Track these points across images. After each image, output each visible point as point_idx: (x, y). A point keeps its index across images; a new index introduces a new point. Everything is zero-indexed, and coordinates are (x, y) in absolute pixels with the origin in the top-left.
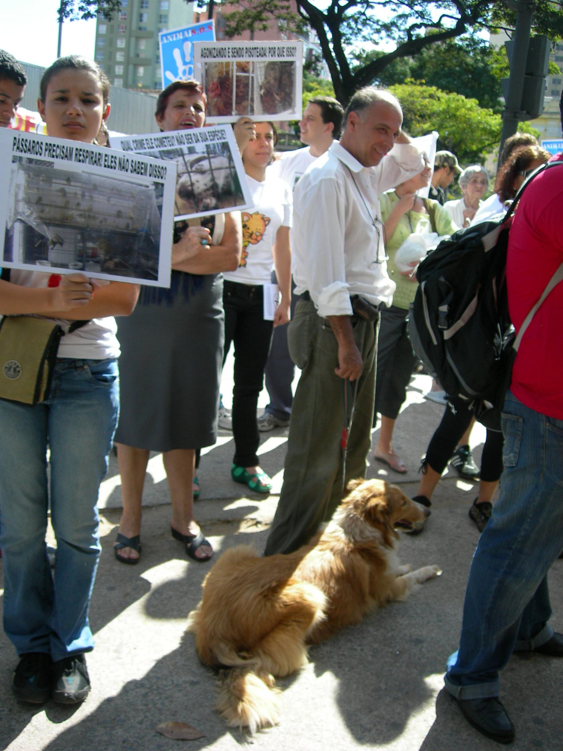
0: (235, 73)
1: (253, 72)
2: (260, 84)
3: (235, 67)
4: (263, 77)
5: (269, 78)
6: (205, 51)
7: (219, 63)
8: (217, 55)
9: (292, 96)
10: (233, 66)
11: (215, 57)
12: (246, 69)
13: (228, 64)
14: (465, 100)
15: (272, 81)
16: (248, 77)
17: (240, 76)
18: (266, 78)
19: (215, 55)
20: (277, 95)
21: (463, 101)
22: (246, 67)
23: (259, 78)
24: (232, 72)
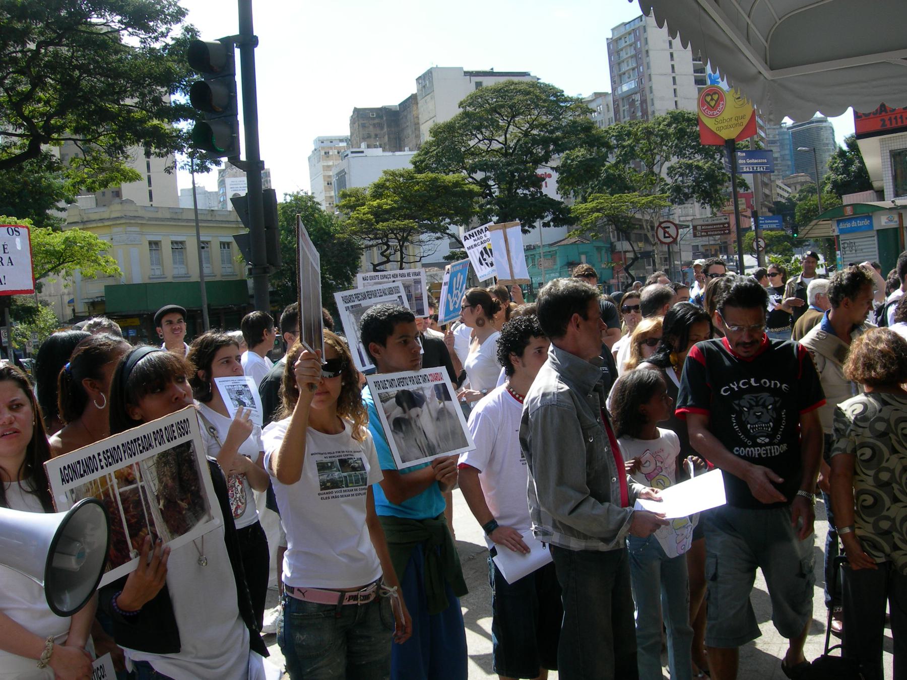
0: (118, 490)
1: (141, 480)
2: (156, 494)
3: (115, 481)
4: (156, 482)
5: (164, 479)
6: (66, 472)
7: (90, 482)
8: (85, 471)
9: (202, 494)
10: (111, 481)
11: (82, 476)
12: (130, 478)
13: (103, 480)
15: (170, 483)
16: (137, 488)
17: (126, 491)
18: (160, 481)
19: (82, 472)
20: (182, 500)
22: (129, 474)
23: (152, 485)
24: (113, 490)
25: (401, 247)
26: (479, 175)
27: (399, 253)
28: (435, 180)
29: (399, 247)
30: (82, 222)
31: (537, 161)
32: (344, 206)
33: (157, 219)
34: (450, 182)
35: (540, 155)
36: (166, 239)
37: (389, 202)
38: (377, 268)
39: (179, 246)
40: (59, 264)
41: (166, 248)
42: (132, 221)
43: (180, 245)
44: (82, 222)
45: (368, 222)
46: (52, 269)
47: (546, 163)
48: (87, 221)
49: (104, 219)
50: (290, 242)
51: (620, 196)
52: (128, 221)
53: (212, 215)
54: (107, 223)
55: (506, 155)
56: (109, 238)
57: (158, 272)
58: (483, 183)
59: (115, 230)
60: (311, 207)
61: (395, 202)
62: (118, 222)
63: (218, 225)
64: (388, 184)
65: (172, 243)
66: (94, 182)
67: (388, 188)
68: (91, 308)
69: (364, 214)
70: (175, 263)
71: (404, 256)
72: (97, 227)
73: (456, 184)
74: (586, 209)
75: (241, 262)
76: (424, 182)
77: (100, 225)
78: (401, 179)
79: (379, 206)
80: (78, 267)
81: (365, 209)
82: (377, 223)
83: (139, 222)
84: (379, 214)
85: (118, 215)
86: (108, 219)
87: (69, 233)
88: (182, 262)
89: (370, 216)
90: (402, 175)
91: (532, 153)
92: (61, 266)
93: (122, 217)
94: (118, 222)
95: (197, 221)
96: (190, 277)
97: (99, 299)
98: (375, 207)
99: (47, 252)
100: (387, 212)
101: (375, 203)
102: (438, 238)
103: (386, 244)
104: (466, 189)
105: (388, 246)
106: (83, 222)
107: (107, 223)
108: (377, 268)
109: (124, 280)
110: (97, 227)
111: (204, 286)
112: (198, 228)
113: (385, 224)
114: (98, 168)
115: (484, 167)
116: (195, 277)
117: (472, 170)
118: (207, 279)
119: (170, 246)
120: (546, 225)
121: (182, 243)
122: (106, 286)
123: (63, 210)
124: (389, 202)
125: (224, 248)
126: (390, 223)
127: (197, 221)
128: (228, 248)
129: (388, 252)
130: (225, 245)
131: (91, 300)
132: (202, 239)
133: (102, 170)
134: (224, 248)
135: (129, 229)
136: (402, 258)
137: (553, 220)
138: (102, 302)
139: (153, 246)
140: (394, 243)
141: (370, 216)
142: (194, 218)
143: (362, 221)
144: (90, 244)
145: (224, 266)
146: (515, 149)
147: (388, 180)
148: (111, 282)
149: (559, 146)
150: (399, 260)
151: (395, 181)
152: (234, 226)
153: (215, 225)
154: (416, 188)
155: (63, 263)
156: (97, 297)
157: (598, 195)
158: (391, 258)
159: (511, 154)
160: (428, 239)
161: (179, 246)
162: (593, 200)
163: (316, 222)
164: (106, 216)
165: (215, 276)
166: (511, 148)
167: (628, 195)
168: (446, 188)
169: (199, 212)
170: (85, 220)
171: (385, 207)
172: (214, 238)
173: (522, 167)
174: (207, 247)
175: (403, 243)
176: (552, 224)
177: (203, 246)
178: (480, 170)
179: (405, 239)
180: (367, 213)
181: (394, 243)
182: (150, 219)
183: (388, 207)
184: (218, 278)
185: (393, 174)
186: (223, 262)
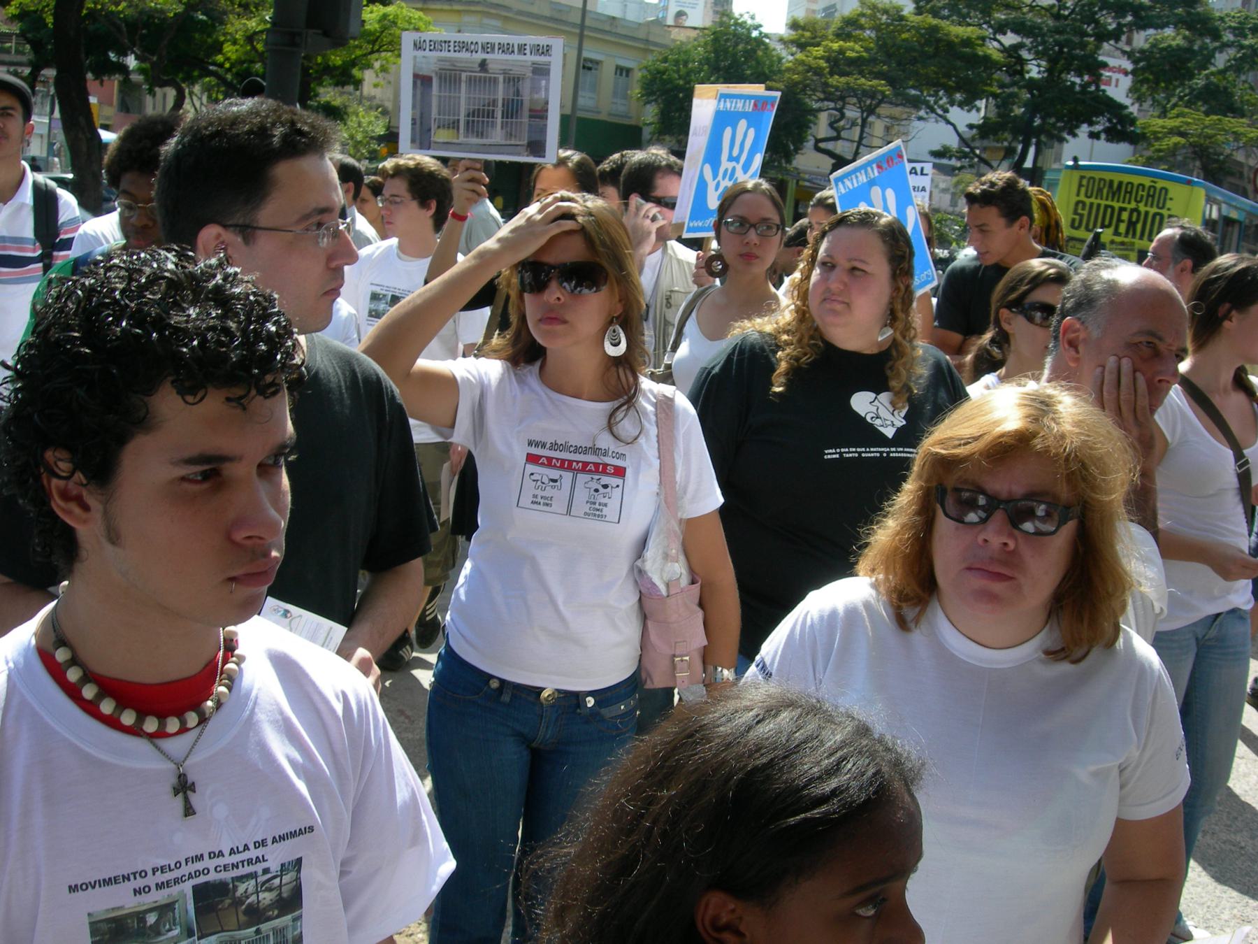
25: (864, 121)
26: (1010, 39)
27: (857, 130)
28: (934, 29)
29: (859, 121)
31: (1103, 36)
32: (792, 42)
33: (530, 15)
34: (957, 37)
35: (1110, 28)
38: (822, 145)
40: (372, 52)
42: (493, 11)
45: (818, 72)
47: (1116, 42)
51: (1219, 120)
52: (486, 9)
53: (611, 24)
55: (1057, 17)
58: (1012, 51)
64: (863, 20)
69: (816, 58)
71: (865, 135)
72: (441, 10)
73: (967, 42)
74: (1163, 127)
76: (917, 29)
78: (885, 17)
79: (841, 51)
81: (818, 51)
82: (832, 74)
84: (837, 63)
89: (823, 64)
90: (886, 12)
91: (1097, 22)
92: (375, 56)
95: (582, 26)
98: (834, 51)
101: (835, 46)
103: (841, 110)
104: (980, 53)
105: (843, 116)
108: (822, 145)
110: (441, 10)
112: (581, 37)
113: (843, 80)
115: (1019, 28)
117: (1001, 28)
118: (580, 114)
120: (1094, 136)
124: (857, 47)
125: (621, 74)
126: (850, 79)
127: (582, 26)
129: (842, 123)
130: (623, 71)
132: (586, 54)
134: (621, 74)
135: (486, 21)
136: (861, 138)
137: (1107, 131)
140: (852, 113)
141: (823, 64)
142: (578, 21)
143: (810, 69)
145: (615, 101)
146: (1073, 11)
147: (863, 15)
149: (1141, 18)
150: (857, 139)
151: (873, 17)
152: (642, 46)
154: (904, 36)
155: (378, 51)
157: (1186, 110)
158: (843, 134)
159: (1066, 18)
162: (1178, 116)
163: (758, 63)
165: (599, 113)
166: (1068, 8)
167: (1232, 120)
168: (950, 44)
171: (850, 54)
173: (1076, 39)
174: (596, 69)
175: (867, 117)
176: (1103, 136)
178: (1013, 31)
179: (871, 111)
180: (820, 58)
181: (852, 113)
182: (520, 13)
184: (603, 117)
185: (874, 7)
186: (615, 94)
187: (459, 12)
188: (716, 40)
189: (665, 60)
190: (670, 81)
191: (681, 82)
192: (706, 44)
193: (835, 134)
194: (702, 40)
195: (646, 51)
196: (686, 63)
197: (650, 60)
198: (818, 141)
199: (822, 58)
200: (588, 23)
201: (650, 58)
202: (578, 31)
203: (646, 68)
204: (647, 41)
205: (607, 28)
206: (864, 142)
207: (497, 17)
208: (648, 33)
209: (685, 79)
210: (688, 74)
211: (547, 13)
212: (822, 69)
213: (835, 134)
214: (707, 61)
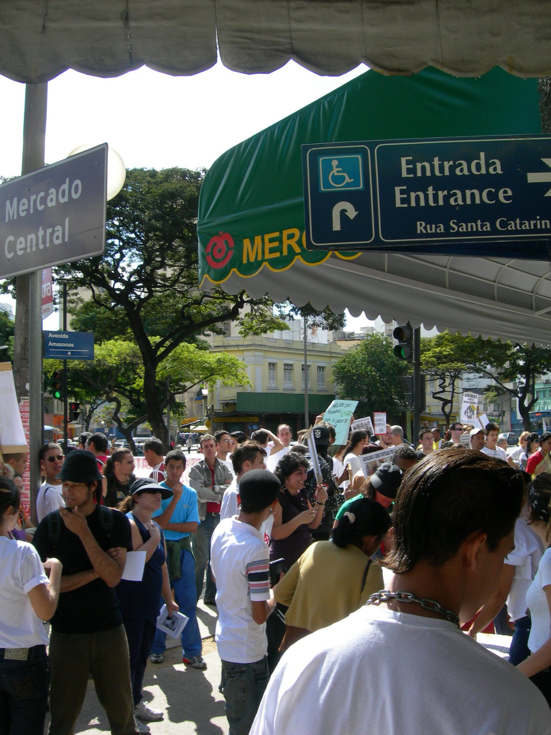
14: (189, 345)
21: (187, 347)
29: (451, 382)
30: (224, 346)
33: (275, 347)
36: (281, 360)
37: (447, 349)
38: (436, 395)
39: (288, 367)
41: (280, 368)
43: (289, 366)
44: (224, 346)
46: (205, 378)
48: (227, 346)
49: (239, 345)
50: (370, 371)
53: (313, 347)
54: (241, 349)
56: (242, 359)
57: (273, 385)
59: (246, 353)
60: (386, 345)
61: (452, 350)
62: (249, 348)
63: (317, 354)
65: (285, 365)
66: (258, 329)
67: (446, 339)
68: (225, 408)
70: (285, 379)
71: (455, 388)
75: (333, 382)
77: (236, 349)
79: (440, 352)
80: (222, 377)
82: (439, 364)
83: (264, 349)
85: (250, 343)
86: (242, 346)
87: (219, 355)
88: (290, 379)
93: (251, 345)
94: (249, 348)
95: (305, 350)
96: (295, 390)
97: (232, 401)
99: (205, 368)
100: (445, 357)
101: (437, 350)
102: (480, 377)
106: (225, 347)
107: (241, 349)
108: (436, 395)
109: (249, 390)
110: (234, 351)
111: (307, 399)
112: (306, 355)
113: (443, 365)
114: (262, 321)
116: (299, 391)
118: (309, 393)
119: (283, 367)
121: (291, 365)
122: (238, 393)
123: (208, 335)
125: (320, 371)
127: (305, 350)
128: (323, 371)
130: (321, 369)
131: (226, 402)
132: (308, 363)
133: (263, 321)
134: (320, 371)
135: (257, 353)
138: (234, 404)
139: (271, 366)
142: (303, 348)
144: (233, 364)
148: (240, 390)
152: (329, 355)
153: (314, 354)
155: (213, 375)
156: (230, 400)
160: (473, 377)
161: (288, 367)
164: (241, 343)
165: (312, 391)
169: (307, 344)
170: (226, 345)
172: (314, 362)
174: (308, 370)
175: (455, 380)
177: (305, 368)
180: (431, 357)
183: (447, 353)
187: (242, 350)
188: (367, 348)
189: (344, 361)
190: (349, 371)
191: (354, 371)
192: (362, 350)
193: (442, 389)
194: (359, 348)
195: (330, 357)
196: (355, 362)
197: (335, 361)
198: (434, 394)
199: (433, 357)
200: (308, 349)
201: (336, 360)
202: (304, 353)
203: (334, 366)
204: (331, 352)
205: (311, 349)
206: (455, 391)
207: (262, 351)
208: (331, 348)
209: (356, 370)
210: (357, 367)
211: (283, 346)
212: (432, 361)
213: (442, 389)
214: (363, 360)
